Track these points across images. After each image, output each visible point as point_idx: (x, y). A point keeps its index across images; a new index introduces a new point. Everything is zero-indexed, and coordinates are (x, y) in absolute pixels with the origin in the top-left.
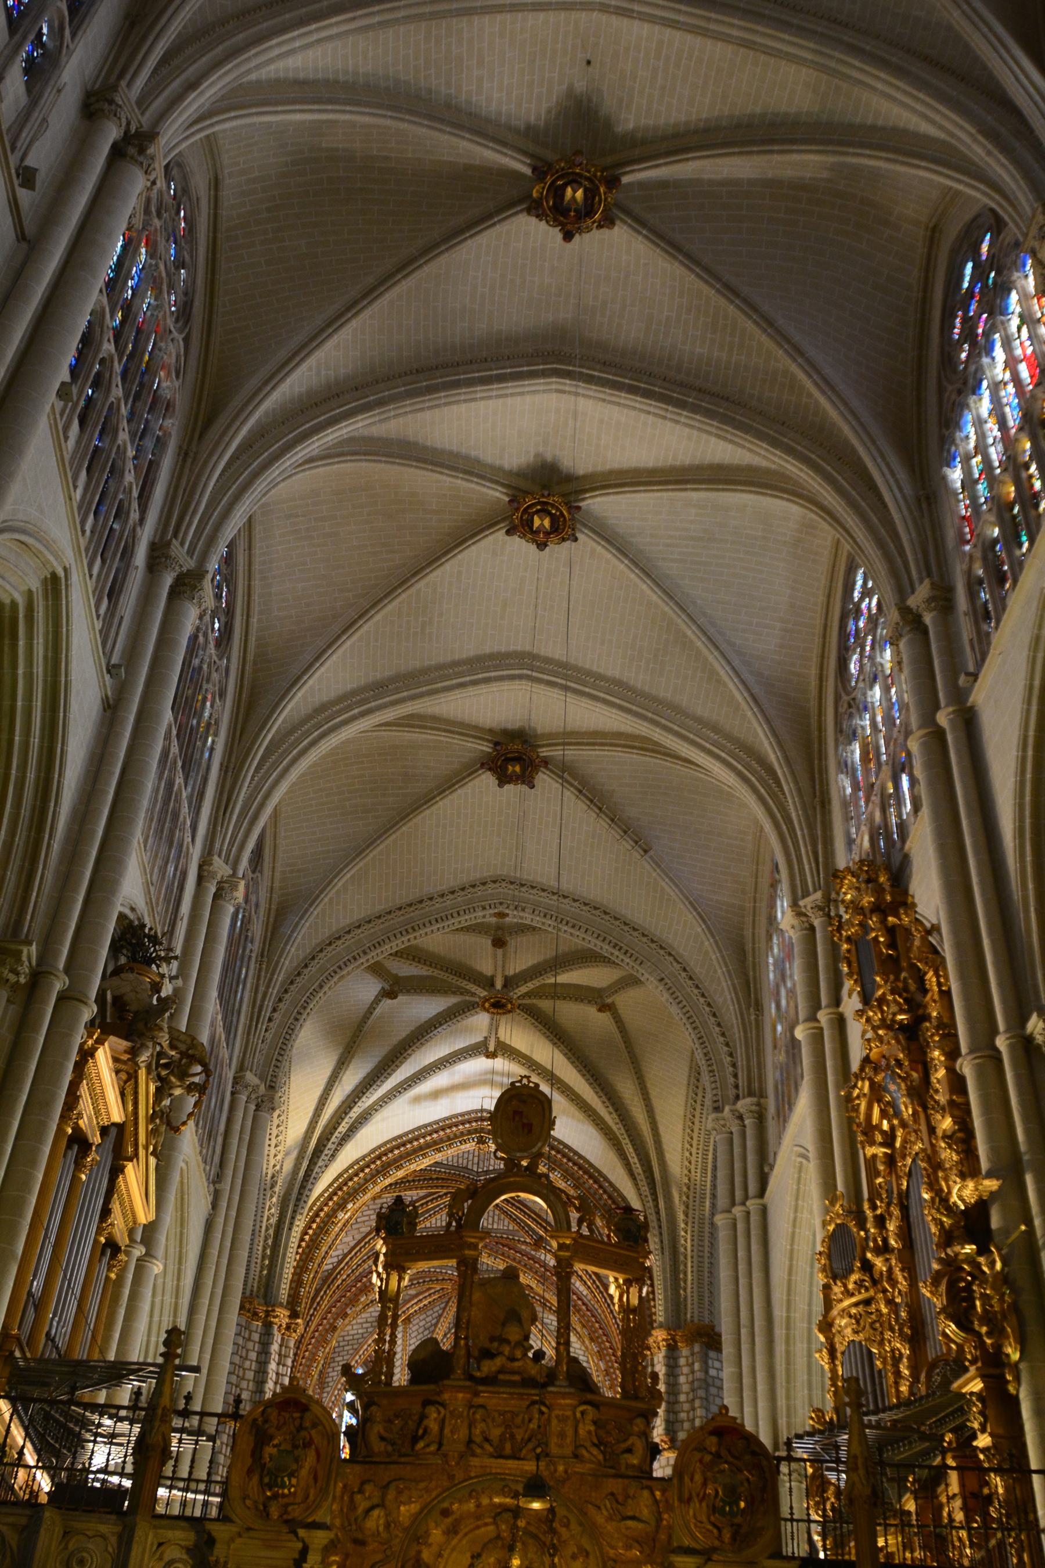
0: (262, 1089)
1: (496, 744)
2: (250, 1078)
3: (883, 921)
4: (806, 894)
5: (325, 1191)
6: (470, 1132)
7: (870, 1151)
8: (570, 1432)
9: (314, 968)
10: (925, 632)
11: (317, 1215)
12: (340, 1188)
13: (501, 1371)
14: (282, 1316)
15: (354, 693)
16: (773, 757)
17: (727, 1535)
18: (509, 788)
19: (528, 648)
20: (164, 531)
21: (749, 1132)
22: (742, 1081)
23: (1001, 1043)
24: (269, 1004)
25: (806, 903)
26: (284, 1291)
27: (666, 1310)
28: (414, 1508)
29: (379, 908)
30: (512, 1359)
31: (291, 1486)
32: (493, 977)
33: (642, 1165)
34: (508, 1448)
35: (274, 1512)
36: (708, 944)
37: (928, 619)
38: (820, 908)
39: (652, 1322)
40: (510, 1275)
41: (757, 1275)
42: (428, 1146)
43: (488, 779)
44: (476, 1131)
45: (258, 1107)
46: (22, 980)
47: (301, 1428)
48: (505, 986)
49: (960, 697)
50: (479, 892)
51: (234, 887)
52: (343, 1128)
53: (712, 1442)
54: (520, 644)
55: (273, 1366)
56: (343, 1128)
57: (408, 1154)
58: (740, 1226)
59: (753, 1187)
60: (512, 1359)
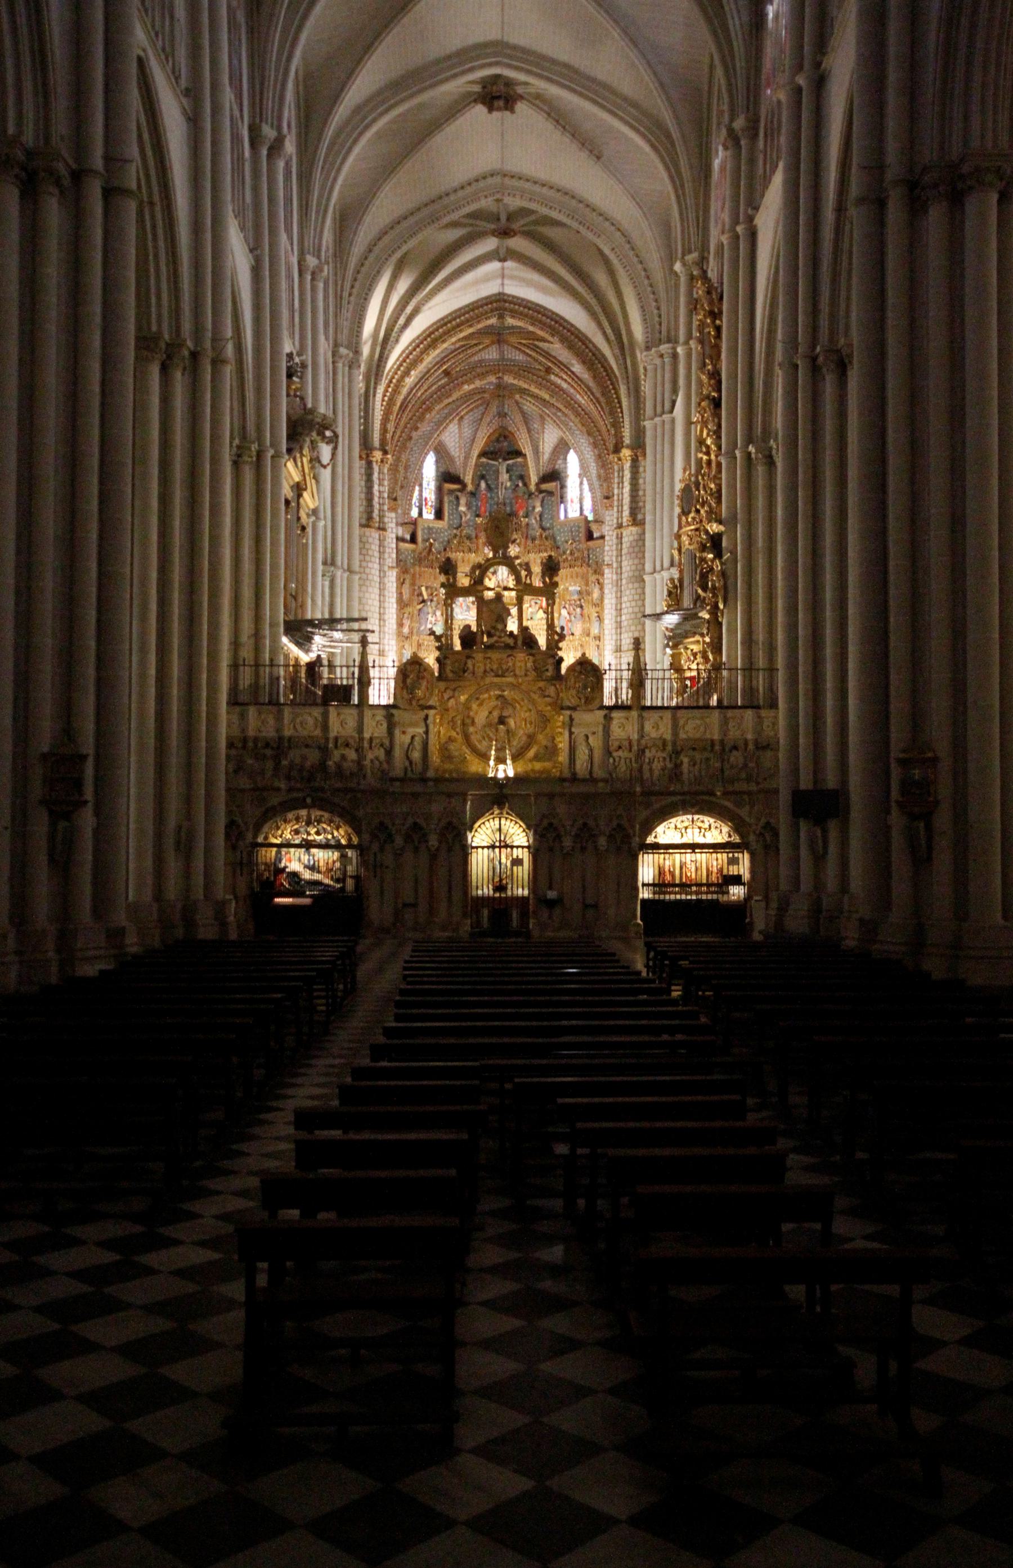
0: (351, 355)
1: (484, 87)
2: (343, 351)
3: (713, 322)
4: (690, 252)
5: (395, 363)
6: (492, 311)
7: (700, 455)
8: (523, 665)
9: (372, 257)
10: (740, 147)
11: (391, 382)
12: (404, 361)
13: (496, 642)
14: (378, 455)
15: (379, 93)
16: (676, 135)
17: (583, 701)
18: (496, 114)
19: (499, 37)
20: (254, 117)
21: (667, 368)
22: (664, 333)
23: (738, 453)
24: (346, 294)
25: (691, 258)
26: (376, 443)
27: (631, 435)
28: (466, 696)
29: (411, 206)
30: (500, 637)
31: (419, 693)
32: (498, 214)
33: (615, 335)
34: (500, 672)
35: (414, 703)
36: (644, 225)
37: (743, 143)
38: (697, 264)
39: (622, 442)
40: (499, 597)
41: (667, 463)
42: (462, 324)
43: (480, 109)
44: (496, 309)
45: (350, 367)
46: (254, 459)
47: (419, 672)
48: (508, 219)
49: (750, 219)
50: (482, 184)
51: (322, 271)
52: (402, 321)
53: (578, 668)
54: (493, 34)
55: (376, 487)
56: (402, 321)
57: (449, 331)
58: (659, 430)
59: (667, 405)
60: (500, 637)
